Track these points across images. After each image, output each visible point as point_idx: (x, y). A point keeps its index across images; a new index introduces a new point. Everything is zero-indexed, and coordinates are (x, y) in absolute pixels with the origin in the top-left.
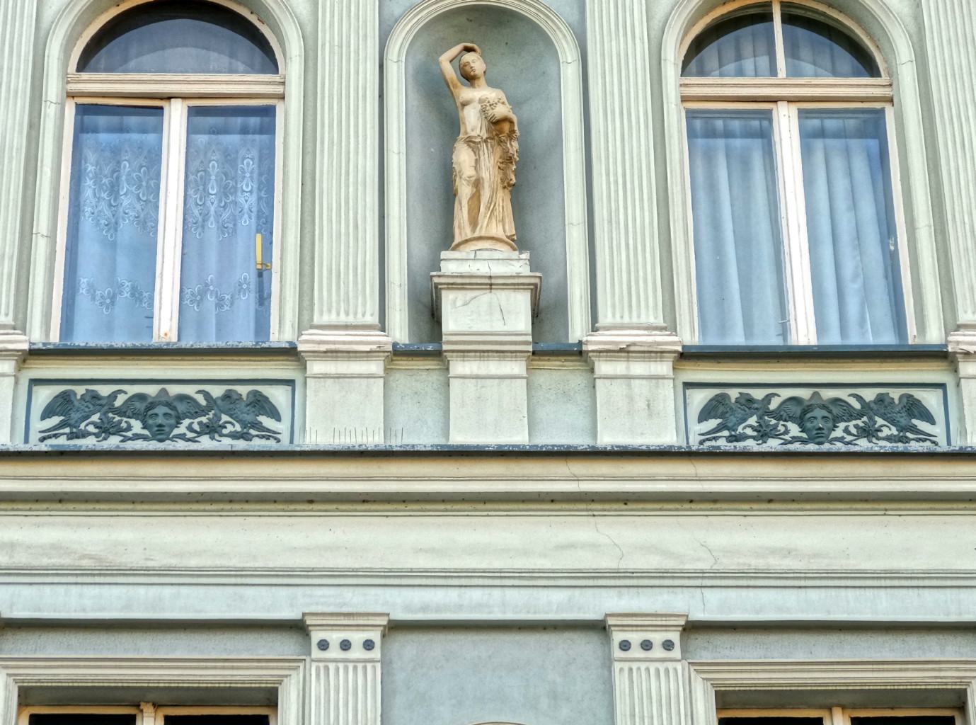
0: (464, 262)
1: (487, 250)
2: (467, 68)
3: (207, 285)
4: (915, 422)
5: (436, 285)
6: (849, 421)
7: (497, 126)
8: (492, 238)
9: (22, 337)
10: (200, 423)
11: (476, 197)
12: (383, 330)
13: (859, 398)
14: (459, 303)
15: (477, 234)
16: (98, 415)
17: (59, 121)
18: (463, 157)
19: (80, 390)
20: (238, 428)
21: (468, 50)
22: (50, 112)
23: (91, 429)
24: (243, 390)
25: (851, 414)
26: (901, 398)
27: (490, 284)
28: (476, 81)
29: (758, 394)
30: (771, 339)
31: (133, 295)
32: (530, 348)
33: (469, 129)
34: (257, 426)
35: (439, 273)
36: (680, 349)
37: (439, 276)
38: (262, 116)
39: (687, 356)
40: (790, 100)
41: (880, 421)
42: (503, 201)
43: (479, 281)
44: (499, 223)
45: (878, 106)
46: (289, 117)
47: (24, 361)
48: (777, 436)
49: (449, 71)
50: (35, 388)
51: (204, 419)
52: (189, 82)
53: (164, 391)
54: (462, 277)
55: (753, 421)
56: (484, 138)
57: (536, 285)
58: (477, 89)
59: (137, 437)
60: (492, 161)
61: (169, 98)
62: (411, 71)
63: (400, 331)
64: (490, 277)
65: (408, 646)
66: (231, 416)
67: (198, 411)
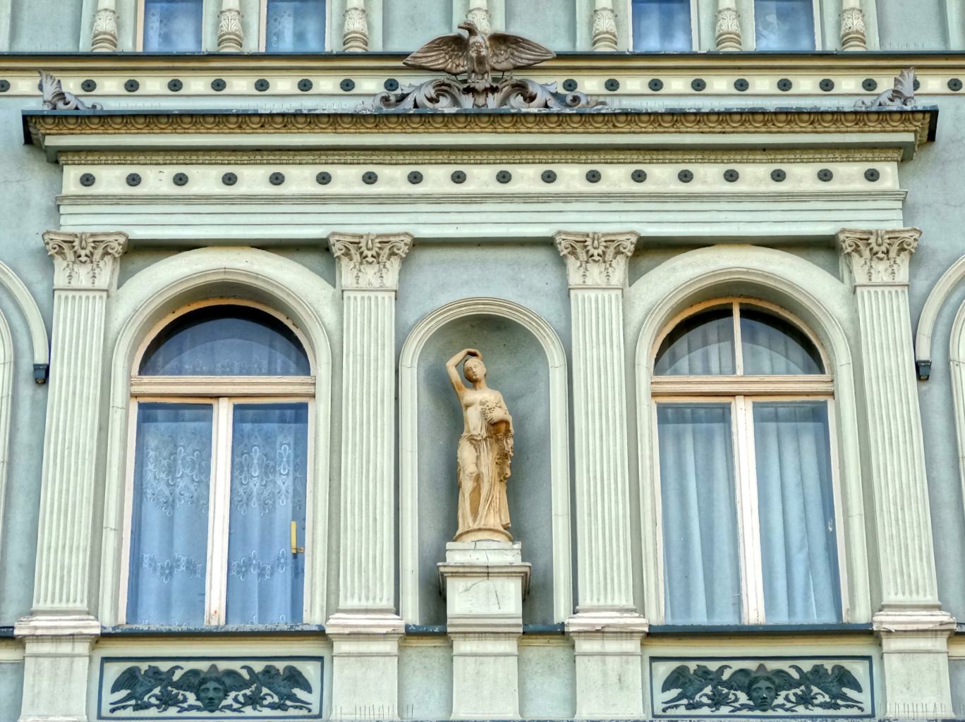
0: (466, 552)
1: (485, 540)
2: (470, 373)
3: (250, 559)
4: (845, 690)
5: (442, 574)
6: (789, 690)
7: (496, 429)
8: (490, 530)
9: (95, 623)
10: (244, 695)
11: (477, 490)
12: (397, 613)
13: (798, 669)
14: (461, 589)
15: (476, 527)
16: (159, 688)
17: (124, 419)
18: (466, 453)
19: (144, 666)
20: (276, 699)
21: (474, 355)
22: (116, 418)
23: (153, 701)
24: (280, 666)
25: (791, 684)
26: (834, 668)
27: (487, 572)
28: (478, 384)
29: (713, 666)
30: (725, 619)
31: (188, 568)
32: (521, 630)
33: (471, 427)
34: (293, 698)
35: (445, 564)
36: (646, 629)
37: (445, 566)
38: (297, 413)
39: (654, 634)
40: (746, 395)
41: (815, 690)
42: (500, 493)
43: (478, 570)
44: (496, 516)
45: (821, 399)
46: (319, 413)
47: (97, 642)
48: (727, 704)
49: (455, 375)
50: (107, 665)
51: (248, 692)
52: (234, 384)
53: (214, 667)
54: (464, 567)
55: (708, 690)
56: (484, 437)
57: (526, 573)
58: (478, 391)
59: (191, 708)
60: (490, 458)
61: (217, 397)
62: (422, 374)
63: (412, 613)
64: (488, 567)
66: (270, 689)
67: (241, 684)
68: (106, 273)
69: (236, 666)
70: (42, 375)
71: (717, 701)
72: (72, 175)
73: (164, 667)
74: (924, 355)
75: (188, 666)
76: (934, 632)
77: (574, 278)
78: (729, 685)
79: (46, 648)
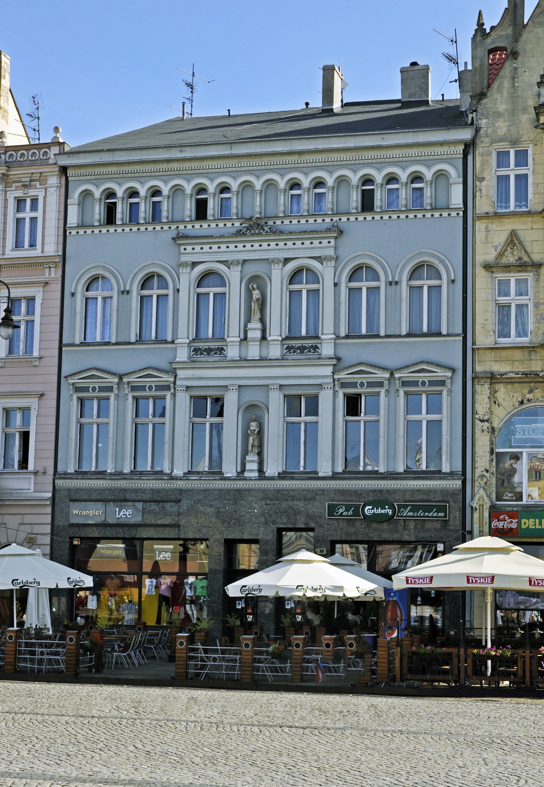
7: (258, 300)
11: (254, 311)
18: (253, 304)
22: (191, 299)
24: (220, 347)
25: (307, 348)
27: (254, 329)
44: (257, 316)
49: (251, 287)
63: (242, 337)
65: (242, 388)
68: (189, 269)
69: (213, 347)
70: (178, 290)
71: (294, 352)
72: (182, 248)
73: (201, 347)
74: (336, 281)
75: (205, 347)
76: (332, 339)
77: (272, 268)
78: (297, 349)
79: (181, 345)
